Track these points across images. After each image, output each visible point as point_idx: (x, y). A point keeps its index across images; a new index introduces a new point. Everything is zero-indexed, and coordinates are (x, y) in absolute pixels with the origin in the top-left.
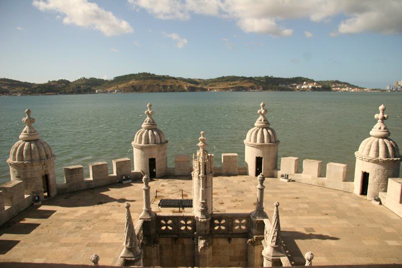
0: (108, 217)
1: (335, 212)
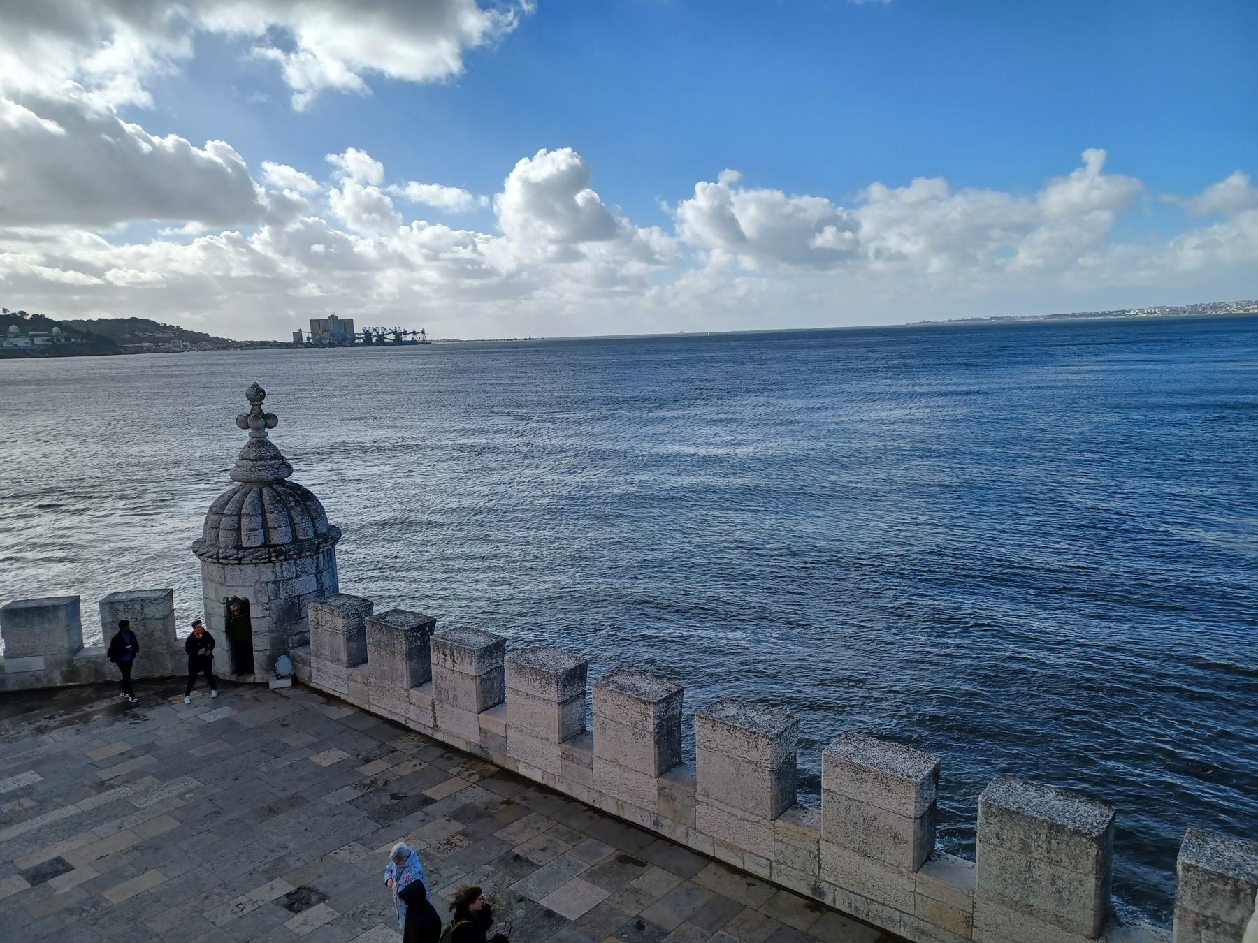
1: (145, 760)
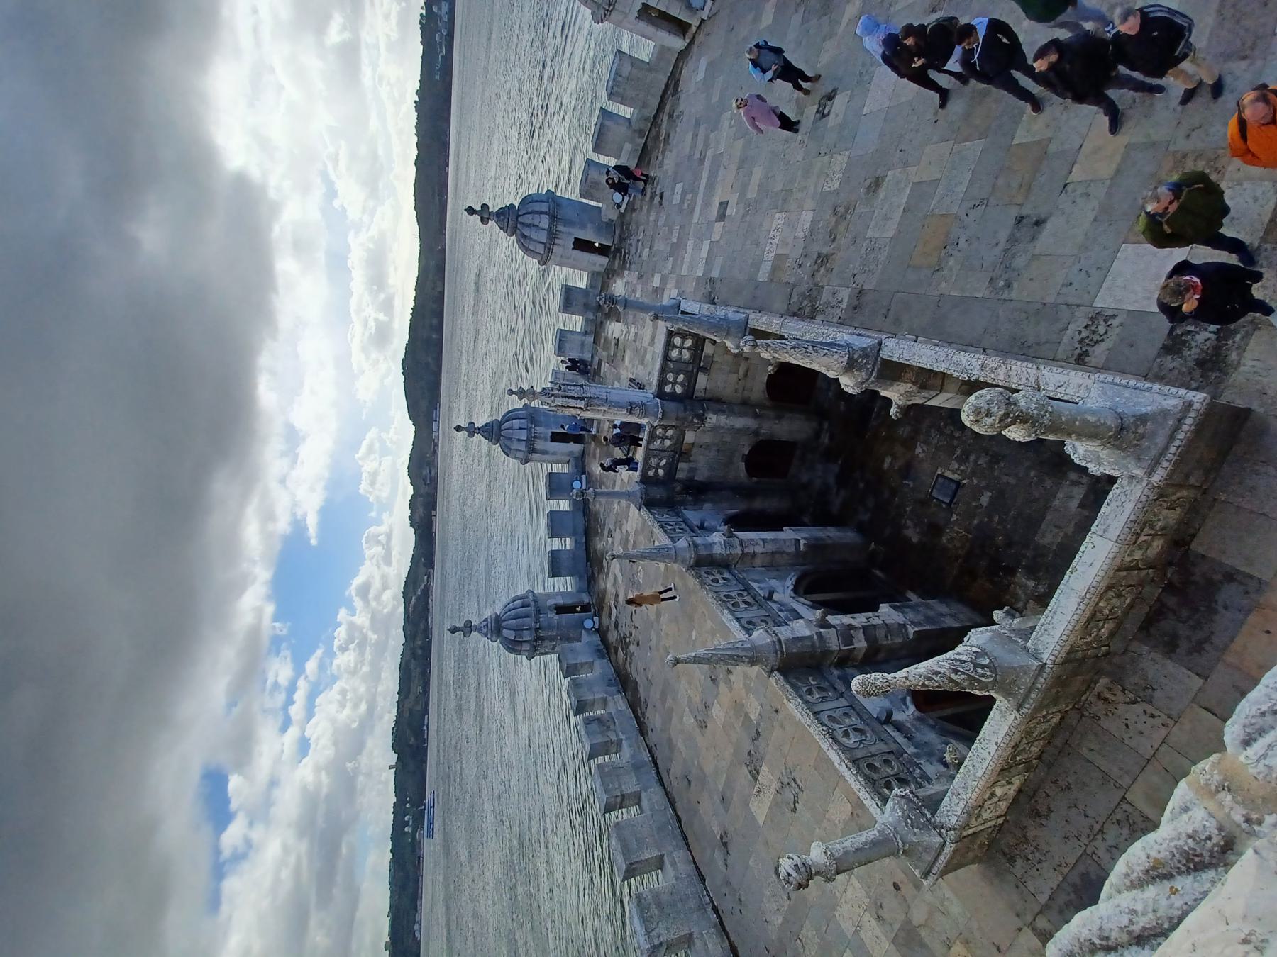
0: (631, 539)
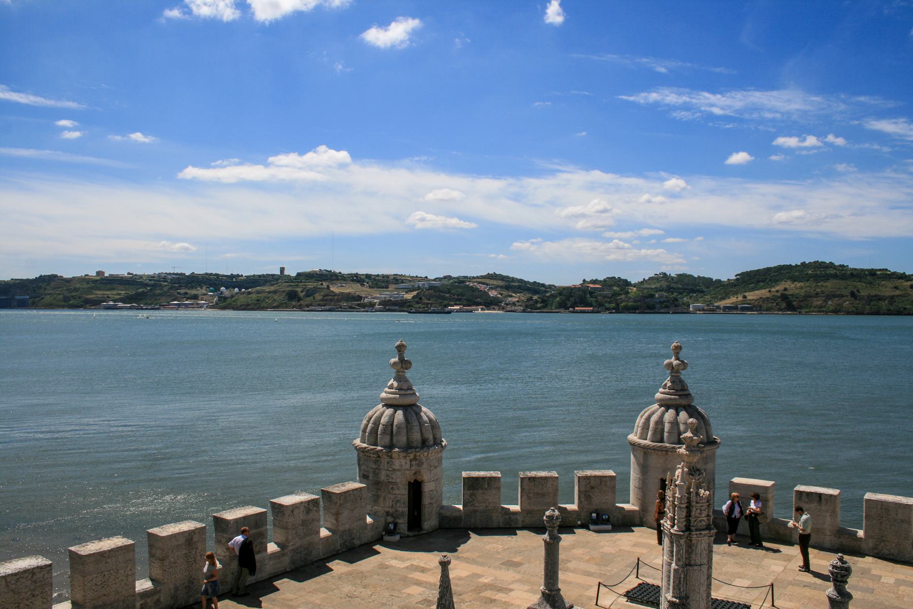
0: (500, 596)
